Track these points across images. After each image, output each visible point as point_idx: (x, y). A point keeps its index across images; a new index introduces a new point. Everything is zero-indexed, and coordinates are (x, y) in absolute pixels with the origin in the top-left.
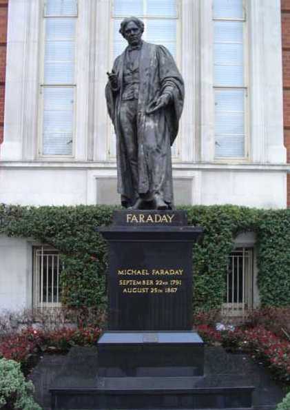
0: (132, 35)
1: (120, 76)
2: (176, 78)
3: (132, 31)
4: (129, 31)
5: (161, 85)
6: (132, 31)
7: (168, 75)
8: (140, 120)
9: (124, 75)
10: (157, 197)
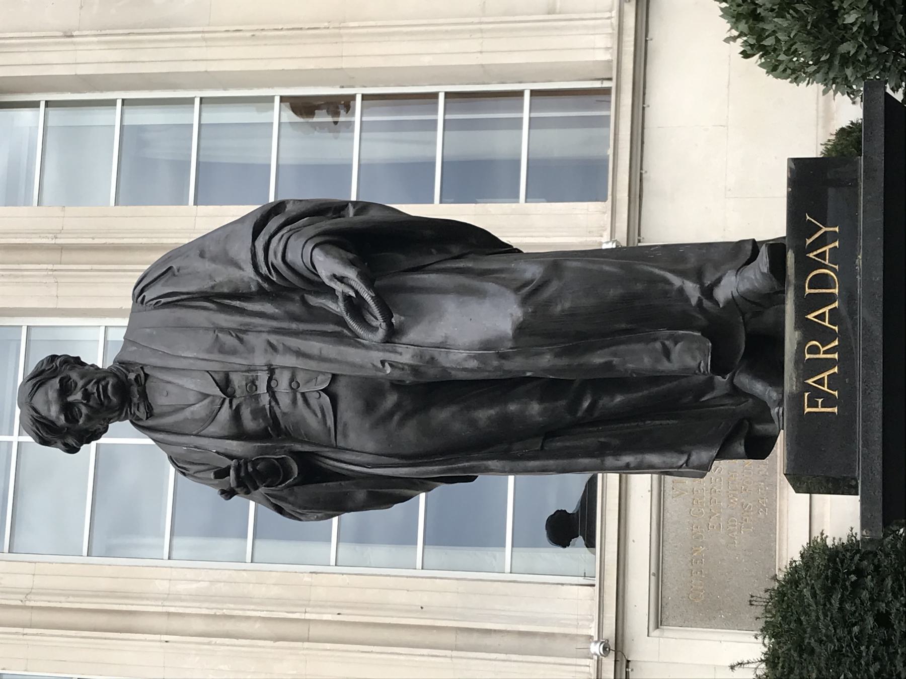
0: (87, 395)
1: (235, 447)
2: (255, 236)
3: (75, 404)
4: (67, 408)
5: (288, 290)
6: (75, 404)
7: (244, 256)
8: (415, 370)
9: (240, 434)
10: (723, 293)
